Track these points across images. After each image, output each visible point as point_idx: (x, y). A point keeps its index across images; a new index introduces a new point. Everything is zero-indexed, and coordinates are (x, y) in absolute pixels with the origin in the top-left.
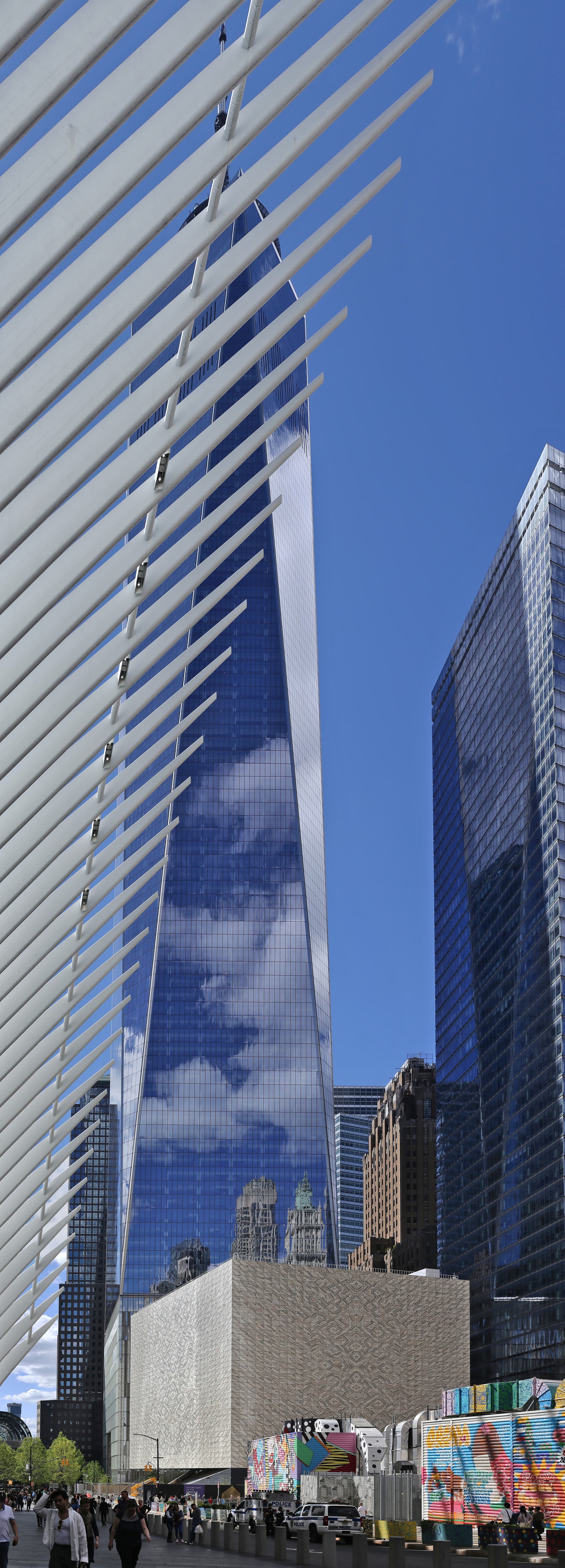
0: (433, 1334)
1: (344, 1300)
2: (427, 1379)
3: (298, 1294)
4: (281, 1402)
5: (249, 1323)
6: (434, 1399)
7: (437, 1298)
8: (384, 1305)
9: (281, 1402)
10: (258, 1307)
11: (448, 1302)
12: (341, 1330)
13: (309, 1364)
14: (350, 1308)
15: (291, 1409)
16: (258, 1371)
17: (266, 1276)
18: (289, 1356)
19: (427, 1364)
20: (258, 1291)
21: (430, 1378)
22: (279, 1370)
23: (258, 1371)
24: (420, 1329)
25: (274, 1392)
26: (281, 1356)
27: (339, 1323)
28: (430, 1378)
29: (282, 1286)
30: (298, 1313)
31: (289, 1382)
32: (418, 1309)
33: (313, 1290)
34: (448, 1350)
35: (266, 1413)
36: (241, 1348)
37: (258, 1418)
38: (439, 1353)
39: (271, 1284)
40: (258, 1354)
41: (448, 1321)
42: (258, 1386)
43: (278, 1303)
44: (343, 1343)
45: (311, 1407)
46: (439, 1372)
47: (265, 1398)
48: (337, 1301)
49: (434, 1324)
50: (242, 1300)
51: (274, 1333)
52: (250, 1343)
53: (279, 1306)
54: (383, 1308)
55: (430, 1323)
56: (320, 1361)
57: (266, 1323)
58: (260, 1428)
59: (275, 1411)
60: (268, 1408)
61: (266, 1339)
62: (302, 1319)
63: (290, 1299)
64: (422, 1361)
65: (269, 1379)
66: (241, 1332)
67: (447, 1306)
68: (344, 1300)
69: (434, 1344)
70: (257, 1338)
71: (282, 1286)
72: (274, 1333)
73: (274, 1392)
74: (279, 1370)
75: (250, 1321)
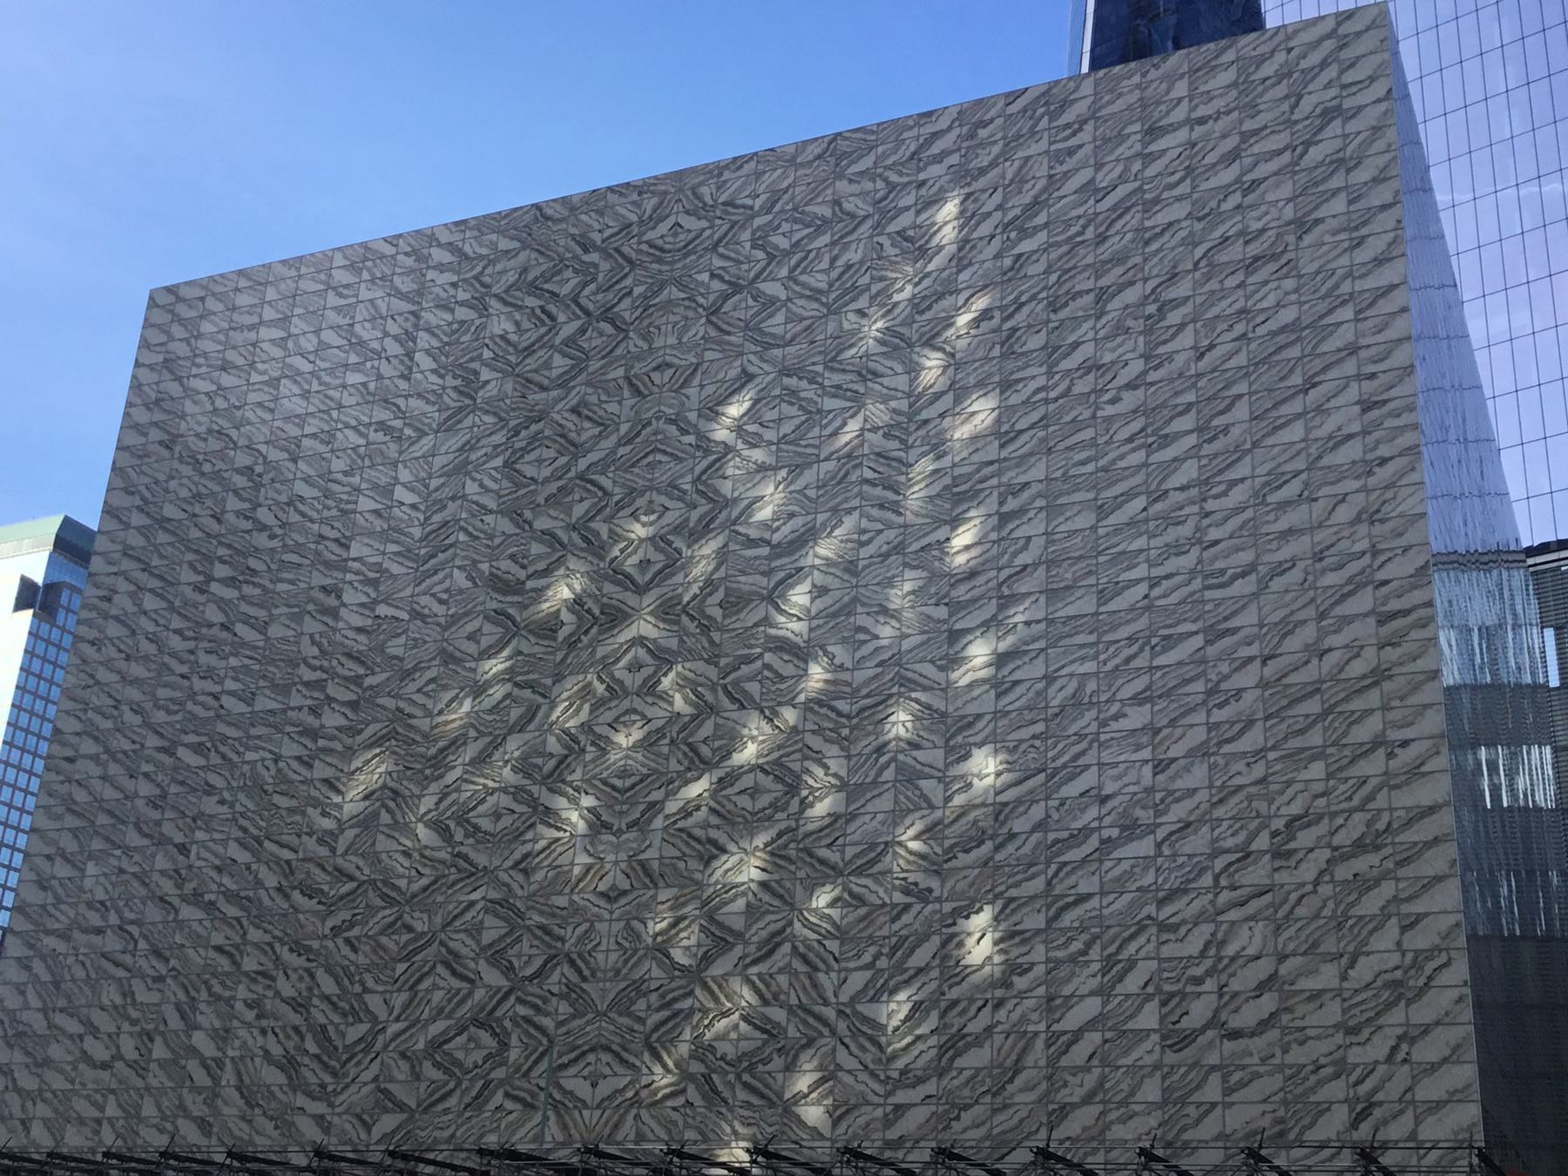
0: (1129, 356)
1: (607, 315)
2: (1084, 604)
3: (393, 348)
4: (234, 851)
5: (163, 522)
6: (1137, 717)
7: (1148, 158)
8: (819, 281)
9: (234, 851)
10: (214, 444)
11: (1233, 156)
12: (577, 450)
13: (396, 647)
14: (635, 343)
15: (271, 881)
16: (160, 716)
17: (269, 314)
18: (311, 626)
19: (1085, 520)
20: (227, 380)
21: (1103, 596)
22: (249, 700)
23: (160, 716)
24: (1035, 342)
25: (210, 805)
26: (275, 631)
27: (570, 422)
28: (1103, 596)
29: (329, 337)
30: (382, 426)
31: (290, 749)
32: (1026, 246)
33: (463, 313)
34: (1241, 411)
35: (154, 913)
36: (113, 630)
37: (113, 943)
38: (1166, 441)
39: (281, 343)
40: (176, 642)
41: (1235, 252)
42: (146, 789)
43: (298, 406)
44: (579, 510)
45: (374, 858)
46: (1177, 549)
47: (162, 841)
48: (568, 330)
49: (1131, 295)
50: (155, 435)
51: (261, 540)
52: (150, 603)
53: (301, 420)
54: (815, 295)
55: (1103, 296)
56: (454, 620)
57: (233, 503)
58: (111, 995)
59: (196, 898)
60: (168, 886)
61: (221, 571)
62: (392, 450)
63: (354, 378)
64: (1052, 510)
65: (198, 749)
66: (127, 564)
67: (1227, 176)
68: (607, 315)
69: (1130, 399)
70: (187, 576)
71: (329, 337)
72: (261, 540)
73: (210, 805)
74: (249, 700)
75: (170, 511)
